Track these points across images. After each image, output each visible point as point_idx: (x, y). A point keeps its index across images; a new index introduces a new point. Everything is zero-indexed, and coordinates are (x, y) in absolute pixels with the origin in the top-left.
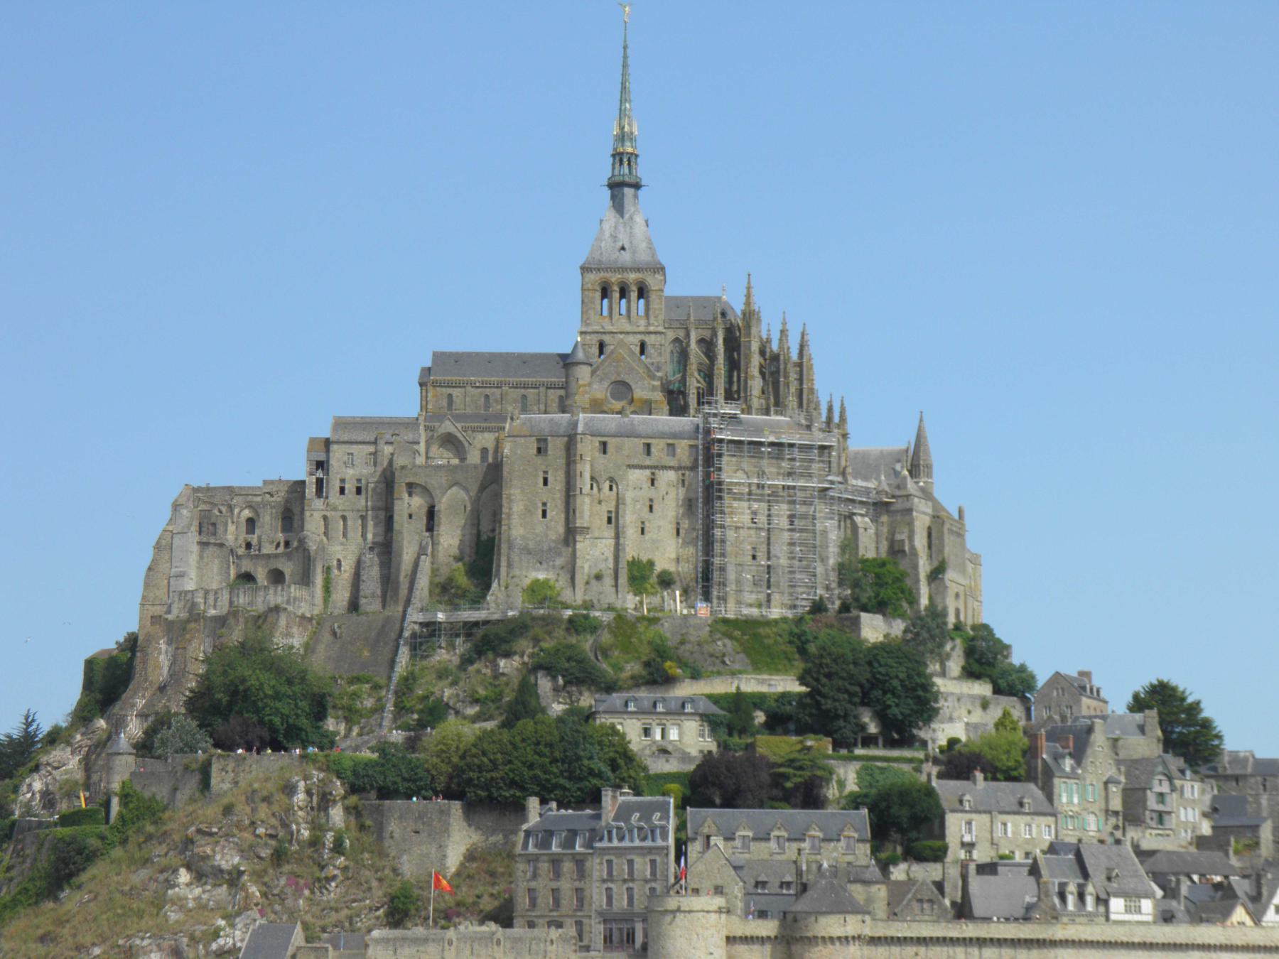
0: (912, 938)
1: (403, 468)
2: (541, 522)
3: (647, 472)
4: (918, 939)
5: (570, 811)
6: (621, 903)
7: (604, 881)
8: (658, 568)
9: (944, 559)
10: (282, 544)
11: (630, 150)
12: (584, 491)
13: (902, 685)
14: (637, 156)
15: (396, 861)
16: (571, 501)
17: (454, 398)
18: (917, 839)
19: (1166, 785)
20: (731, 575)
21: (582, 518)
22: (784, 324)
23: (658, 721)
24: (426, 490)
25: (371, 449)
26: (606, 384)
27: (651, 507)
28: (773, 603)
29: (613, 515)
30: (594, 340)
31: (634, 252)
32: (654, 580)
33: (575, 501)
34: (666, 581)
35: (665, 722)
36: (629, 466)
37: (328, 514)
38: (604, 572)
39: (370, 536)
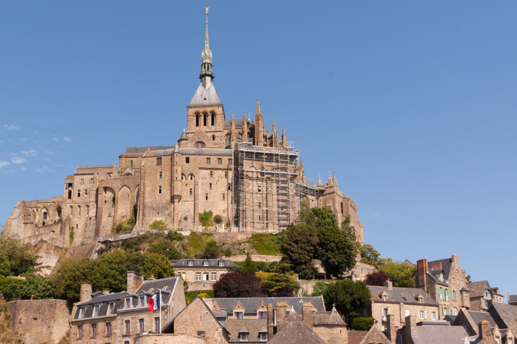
1: (102, 181)
2: (159, 195)
3: (209, 171)
7: (124, 336)
8: (214, 214)
9: (349, 216)
12: (178, 179)
13: (336, 247)
15: (22, 337)
16: (172, 182)
17: (134, 162)
18: (356, 316)
20: (249, 214)
21: (177, 191)
23: (204, 271)
24: (112, 190)
25: (92, 176)
26: (194, 143)
27: (211, 186)
28: (269, 227)
29: (193, 191)
32: (212, 219)
33: (174, 183)
34: (218, 220)
35: (208, 271)
37: (73, 205)
38: (188, 217)
39: (90, 213)
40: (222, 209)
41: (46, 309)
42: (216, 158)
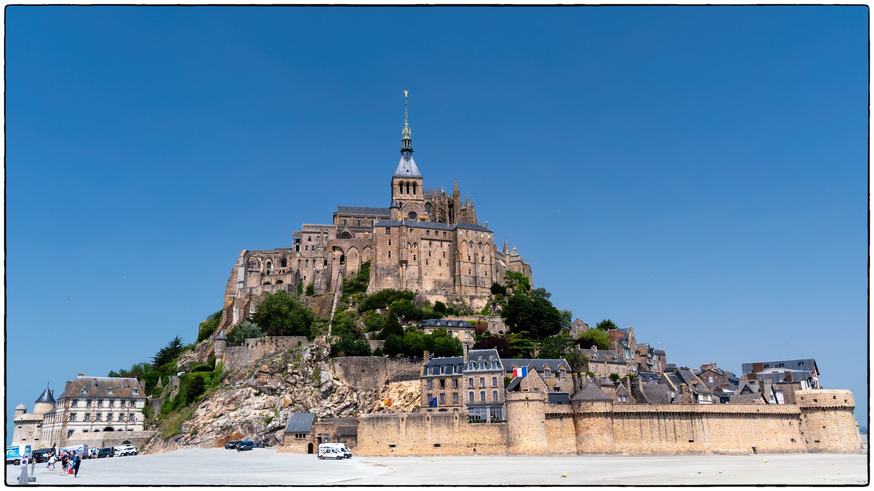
0: (634, 413)
3: (429, 241)
4: (637, 413)
5: (444, 357)
6: (478, 399)
7: (469, 388)
10: (282, 271)
11: (409, 138)
14: (411, 142)
19: (650, 354)
24: (341, 249)
25: (319, 235)
27: (430, 254)
30: (398, 202)
31: (412, 173)
36: (422, 239)
40: (439, 273)
41: (371, 364)
42: (434, 231)
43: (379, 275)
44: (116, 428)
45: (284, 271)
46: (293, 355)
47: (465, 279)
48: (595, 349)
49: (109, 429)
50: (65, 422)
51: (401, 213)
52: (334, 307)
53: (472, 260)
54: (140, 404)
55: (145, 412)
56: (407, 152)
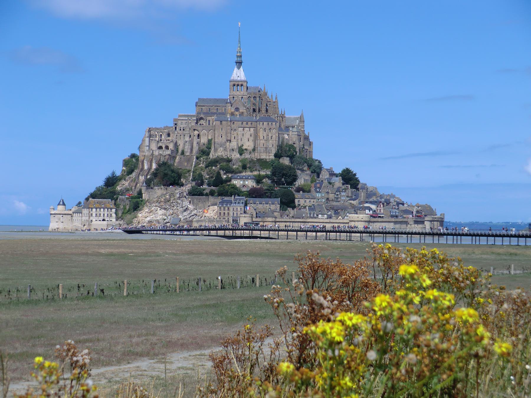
3: (243, 128)
6: (235, 215)
11: (240, 55)
22: (272, 94)
30: (232, 96)
40: (248, 145)
43: (216, 147)
44: (106, 219)
45: (169, 140)
46: (172, 195)
47: (261, 148)
48: (301, 192)
49: (104, 220)
50: (89, 217)
51: (231, 108)
52: (194, 163)
53: (265, 139)
54: (114, 210)
55: (116, 213)
56: (239, 64)
